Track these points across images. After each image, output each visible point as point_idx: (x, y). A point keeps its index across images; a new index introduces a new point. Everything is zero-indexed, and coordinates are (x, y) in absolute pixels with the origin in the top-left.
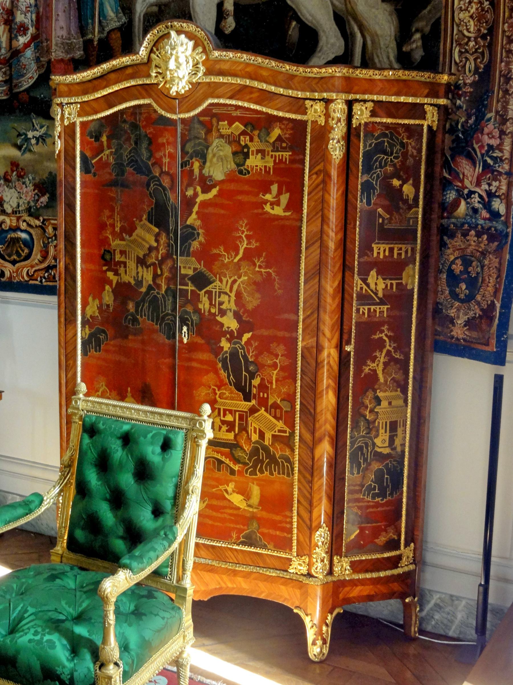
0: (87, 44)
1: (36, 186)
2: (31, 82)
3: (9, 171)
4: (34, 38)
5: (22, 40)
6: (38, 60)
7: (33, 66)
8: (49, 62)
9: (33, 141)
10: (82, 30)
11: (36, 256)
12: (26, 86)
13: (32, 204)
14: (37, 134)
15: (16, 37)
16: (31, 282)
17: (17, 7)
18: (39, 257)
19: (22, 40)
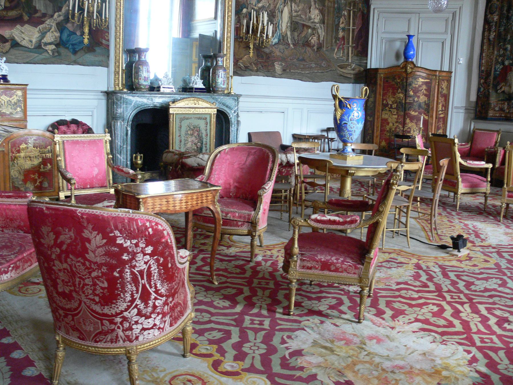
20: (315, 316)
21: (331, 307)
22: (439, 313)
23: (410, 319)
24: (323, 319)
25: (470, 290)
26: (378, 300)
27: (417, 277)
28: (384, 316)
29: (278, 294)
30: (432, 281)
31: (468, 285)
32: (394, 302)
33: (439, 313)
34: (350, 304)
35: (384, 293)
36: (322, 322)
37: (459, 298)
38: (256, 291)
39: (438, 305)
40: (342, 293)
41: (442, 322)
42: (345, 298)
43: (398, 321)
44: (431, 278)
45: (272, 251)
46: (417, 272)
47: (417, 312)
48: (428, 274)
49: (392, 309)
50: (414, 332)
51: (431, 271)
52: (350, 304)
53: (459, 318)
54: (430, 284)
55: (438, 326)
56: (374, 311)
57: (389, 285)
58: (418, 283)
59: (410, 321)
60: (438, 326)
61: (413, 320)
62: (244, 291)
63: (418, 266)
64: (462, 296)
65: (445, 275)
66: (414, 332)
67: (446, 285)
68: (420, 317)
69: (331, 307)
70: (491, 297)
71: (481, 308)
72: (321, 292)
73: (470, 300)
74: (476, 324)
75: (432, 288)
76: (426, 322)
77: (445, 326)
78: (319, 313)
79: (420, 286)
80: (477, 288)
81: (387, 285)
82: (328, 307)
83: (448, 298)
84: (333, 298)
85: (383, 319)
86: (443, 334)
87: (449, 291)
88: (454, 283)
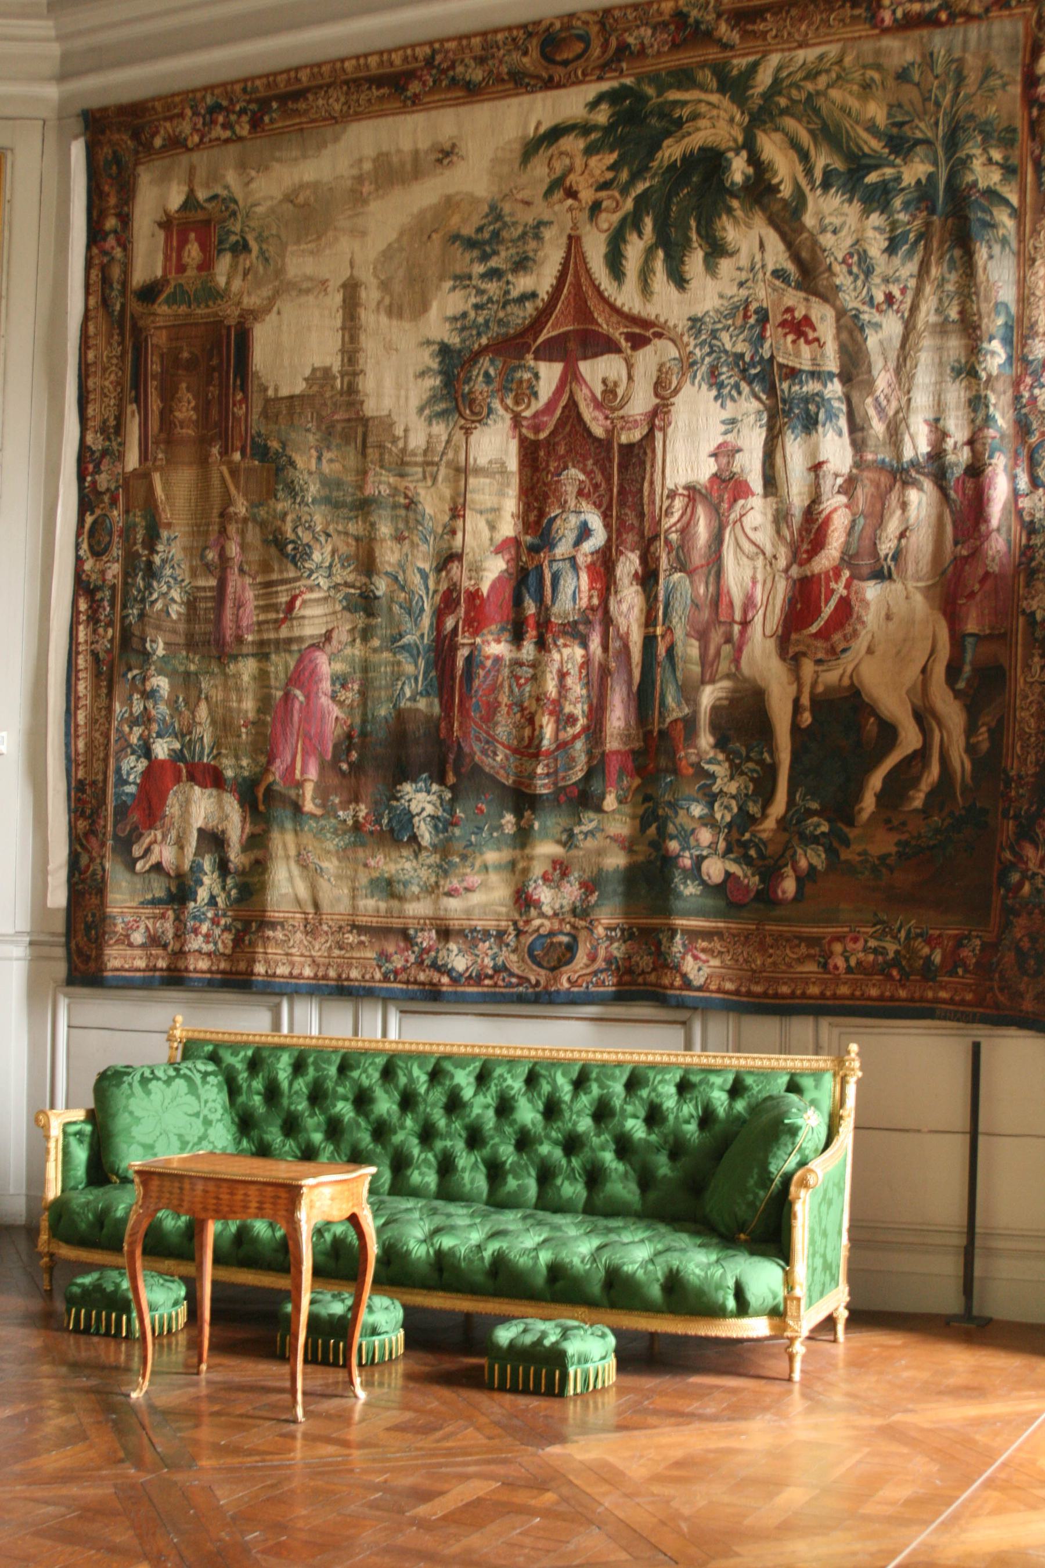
1: (583, 885)
2: (580, 775)
3: (550, 870)
4: (586, 729)
5: (571, 731)
6: (590, 754)
8: (603, 754)
9: (581, 837)
12: (575, 779)
13: (578, 904)
14: (585, 828)
15: (565, 729)
16: (575, 989)
17: (565, 698)
18: (585, 960)
19: (571, 731)
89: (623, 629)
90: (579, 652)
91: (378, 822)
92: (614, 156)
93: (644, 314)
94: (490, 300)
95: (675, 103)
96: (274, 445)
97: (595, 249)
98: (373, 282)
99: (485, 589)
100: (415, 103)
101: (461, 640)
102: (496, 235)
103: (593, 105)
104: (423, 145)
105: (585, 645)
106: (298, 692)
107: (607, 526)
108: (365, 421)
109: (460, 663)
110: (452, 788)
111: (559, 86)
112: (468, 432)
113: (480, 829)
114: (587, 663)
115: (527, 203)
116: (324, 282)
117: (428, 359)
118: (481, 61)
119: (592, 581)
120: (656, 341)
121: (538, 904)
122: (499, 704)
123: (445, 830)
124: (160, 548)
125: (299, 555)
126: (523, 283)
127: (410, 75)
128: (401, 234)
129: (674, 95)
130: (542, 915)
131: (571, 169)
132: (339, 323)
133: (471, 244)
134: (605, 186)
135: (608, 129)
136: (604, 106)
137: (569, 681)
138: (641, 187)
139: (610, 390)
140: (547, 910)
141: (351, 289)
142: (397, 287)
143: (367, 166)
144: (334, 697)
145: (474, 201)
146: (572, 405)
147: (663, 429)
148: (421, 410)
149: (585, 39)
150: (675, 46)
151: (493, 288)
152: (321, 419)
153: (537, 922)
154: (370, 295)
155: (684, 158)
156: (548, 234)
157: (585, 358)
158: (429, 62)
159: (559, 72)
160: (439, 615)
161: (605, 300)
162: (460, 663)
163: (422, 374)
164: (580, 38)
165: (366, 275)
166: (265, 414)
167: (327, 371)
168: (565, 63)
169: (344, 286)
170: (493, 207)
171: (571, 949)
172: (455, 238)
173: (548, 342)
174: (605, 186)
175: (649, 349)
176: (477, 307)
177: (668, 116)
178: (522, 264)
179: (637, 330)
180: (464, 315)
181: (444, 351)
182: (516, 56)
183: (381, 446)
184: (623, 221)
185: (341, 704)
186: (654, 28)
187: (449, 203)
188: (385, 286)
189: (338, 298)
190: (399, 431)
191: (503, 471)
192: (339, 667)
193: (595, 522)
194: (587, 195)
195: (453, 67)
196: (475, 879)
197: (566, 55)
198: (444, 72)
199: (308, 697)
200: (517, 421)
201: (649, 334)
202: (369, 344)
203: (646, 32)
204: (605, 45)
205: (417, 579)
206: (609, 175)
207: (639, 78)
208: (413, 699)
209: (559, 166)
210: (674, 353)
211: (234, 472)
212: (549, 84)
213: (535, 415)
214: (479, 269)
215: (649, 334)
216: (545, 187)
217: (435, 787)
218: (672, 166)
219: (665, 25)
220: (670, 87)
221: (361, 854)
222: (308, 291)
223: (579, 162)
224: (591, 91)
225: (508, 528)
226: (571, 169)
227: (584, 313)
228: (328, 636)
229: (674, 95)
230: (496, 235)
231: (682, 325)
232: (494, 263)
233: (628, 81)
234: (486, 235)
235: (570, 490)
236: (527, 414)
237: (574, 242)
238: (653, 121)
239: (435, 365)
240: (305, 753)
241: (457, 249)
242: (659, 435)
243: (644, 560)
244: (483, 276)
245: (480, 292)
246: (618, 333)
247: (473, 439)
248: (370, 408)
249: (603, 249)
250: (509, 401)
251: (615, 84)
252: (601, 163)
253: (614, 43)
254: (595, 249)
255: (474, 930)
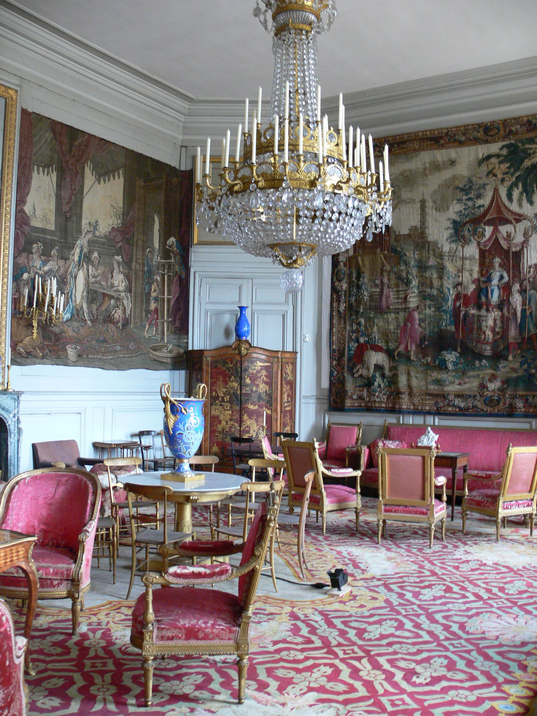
0: (523, 338)
7: (502, 345)
10: (521, 334)
11: (501, 404)
20: (180, 703)
21: (199, 687)
22: (335, 676)
23: (301, 690)
24: (193, 705)
25: (364, 639)
26: (256, 669)
27: (296, 630)
28: (268, 690)
29: (123, 678)
30: (316, 634)
31: (360, 633)
32: (277, 668)
33: (335, 676)
34: (222, 680)
35: (260, 658)
36: (192, 710)
37: (353, 652)
38: (93, 678)
39: (332, 665)
40: (207, 665)
41: (341, 687)
42: (212, 672)
43: (288, 693)
44: (313, 630)
45: (99, 616)
46: (295, 625)
47: (308, 679)
48: (308, 625)
49: (277, 678)
50: (311, 706)
51: (311, 620)
52: (222, 680)
53: (360, 679)
54: (314, 638)
55: (338, 693)
56: (254, 684)
57: (265, 647)
58: (299, 640)
59: (302, 692)
60: (338, 693)
61: (305, 689)
62: (75, 680)
63: (294, 616)
64: (356, 649)
65: (330, 624)
66: (311, 706)
67: (334, 637)
68: (313, 685)
69: (199, 687)
70: (390, 644)
71: (382, 660)
72: (180, 667)
73: (367, 652)
74: (381, 684)
75: (318, 643)
76: (322, 689)
77: (345, 692)
78: (185, 698)
79: (302, 643)
80: (371, 636)
81: (262, 647)
82: (194, 687)
83: (341, 655)
84: (198, 673)
85: (269, 694)
86: (346, 702)
87: (339, 645)
88: (343, 633)
89: (514, 307)
90: (500, 313)
91: (435, 362)
92: (508, 165)
93: (519, 213)
94: (469, 207)
95: (528, 148)
96: (399, 249)
97: (503, 192)
98: (430, 200)
99: (469, 294)
100: (442, 146)
101: (462, 309)
102: (470, 187)
103: (501, 149)
104: (445, 159)
105: (502, 311)
106: (409, 324)
107: (509, 276)
108: (429, 243)
109: (462, 316)
110: (459, 353)
111: (490, 142)
112: (463, 247)
113: (468, 365)
114: (503, 316)
115: (480, 178)
116: (414, 200)
117: (449, 224)
118: (464, 134)
119: (504, 292)
120: (524, 221)
121: (487, 388)
122: (473, 328)
123: (457, 365)
124: (361, 279)
125: (408, 283)
126: (480, 202)
127: (441, 138)
128: (439, 187)
129: (527, 146)
130: (488, 391)
131: (494, 168)
132: (419, 212)
133: (462, 190)
134: (506, 173)
135: (506, 157)
136: (505, 149)
137: (497, 322)
138: (517, 174)
139: (509, 235)
140: (490, 389)
141: (423, 203)
142: (438, 202)
143: (427, 165)
144: (420, 325)
145: (463, 177)
146: (497, 239)
147: (527, 248)
148: (447, 240)
149: (498, 129)
150: (528, 131)
151: (470, 203)
152: (414, 242)
153: (486, 393)
154: (430, 204)
155: (531, 165)
156: (488, 188)
157: (501, 225)
158: (447, 134)
159: (490, 138)
160: (455, 301)
161: (507, 208)
162: (462, 316)
163: (448, 229)
164: (497, 128)
165: (428, 198)
166: (396, 240)
167: (416, 227)
168: (492, 136)
169: (421, 201)
170: (469, 179)
171: (498, 401)
172: (457, 188)
173: (488, 220)
174: (506, 173)
175: (521, 223)
176: (464, 209)
177: (526, 153)
178: (479, 196)
179: (517, 217)
180: (461, 211)
181: (454, 222)
182: (475, 133)
183: (434, 250)
184: (512, 184)
185: (422, 327)
186: (521, 126)
187: (455, 177)
188: (434, 202)
189: (419, 205)
190: (440, 246)
191: (474, 258)
192: (422, 316)
193: (505, 275)
194: (500, 176)
195: (455, 135)
196: (467, 380)
197: (492, 133)
198: (452, 137)
199: (412, 325)
200: (479, 243)
201: (521, 218)
202: (430, 220)
203: (518, 127)
204: (505, 131)
205: (446, 291)
206: (507, 170)
207: (516, 141)
208: (446, 326)
209: (490, 167)
210: (529, 224)
211: (385, 257)
212: (487, 142)
213: (485, 242)
214: (465, 198)
215: (521, 218)
216: (486, 173)
217: (453, 352)
218: (528, 168)
219: (524, 124)
220: (526, 143)
221: (429, 372)
222: (409, 203)
223: (497, 166)
224: (500, 144)
225: (476, 275)
226: (494, 168)
227: (499, 211)
228: (418, 307)
229: (527, 146)
230: (470, 187)
231: (532, 216)
232: (470, 196)
233: (513, 142)
234: (467, 187)
235: (497, 265)
236: (482, 241)
237: (496, 190)
238: (521, 154)
239: (451, 226)
240: (411, 342)
241: (458, 192)
242: (525, 249)
243: (521, 286)
244: (466, 200)
245: (465, 204)
246: (510, 217)
247: (465, 249)
248: (431, 238)
249: (505, 193)
250: (476, 238)
251: (508, 142)
252: (505, 166)
253: (508, 129)
254: (503, 192)
255: (466, 395)
